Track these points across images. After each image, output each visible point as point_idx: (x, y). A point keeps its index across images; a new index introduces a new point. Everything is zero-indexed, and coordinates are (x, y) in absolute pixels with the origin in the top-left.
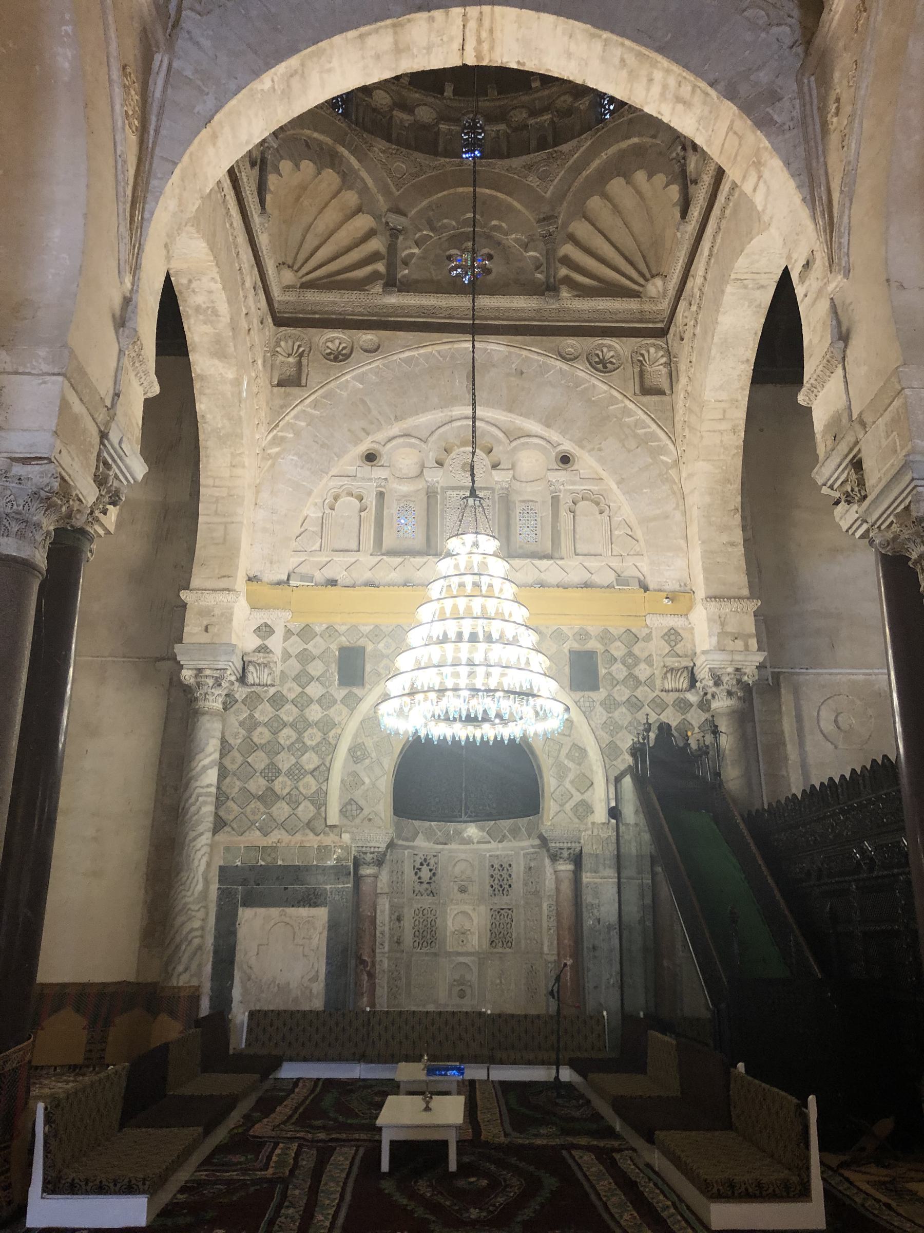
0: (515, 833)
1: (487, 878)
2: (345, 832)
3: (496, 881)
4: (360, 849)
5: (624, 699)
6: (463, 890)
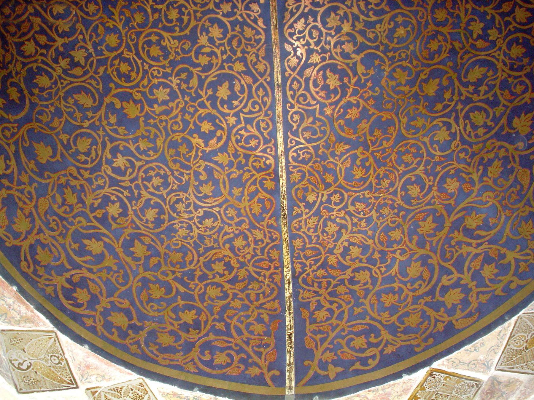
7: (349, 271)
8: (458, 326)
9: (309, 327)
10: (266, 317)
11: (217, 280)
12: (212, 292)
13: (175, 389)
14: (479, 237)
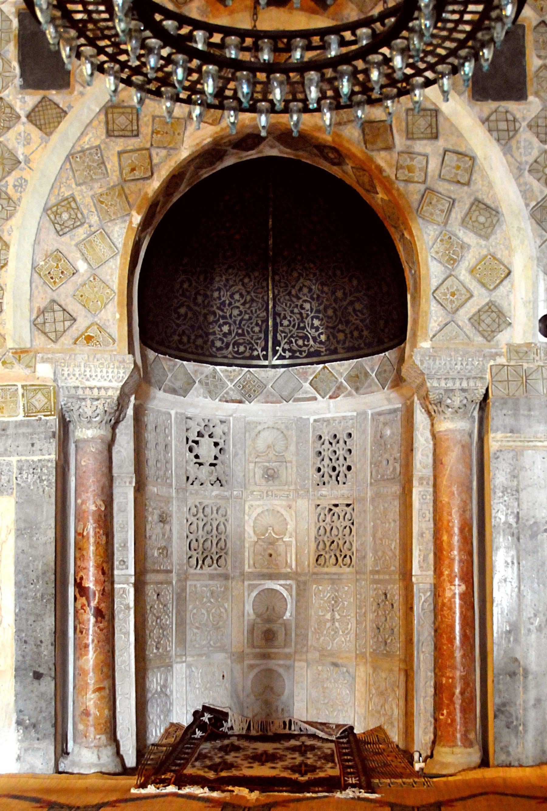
0: (357, 381)
1: (311, 454)
2: (43, 361)
3: (327, 461)
4: (73, 391)
6: (271, 476)
7: (301, 301)
8: (340, 350)
9: (280, 328)
10: (260, 322)
11: (237, 304)
12: (236, 312)
13: (225, 367)
14: (357, 315)
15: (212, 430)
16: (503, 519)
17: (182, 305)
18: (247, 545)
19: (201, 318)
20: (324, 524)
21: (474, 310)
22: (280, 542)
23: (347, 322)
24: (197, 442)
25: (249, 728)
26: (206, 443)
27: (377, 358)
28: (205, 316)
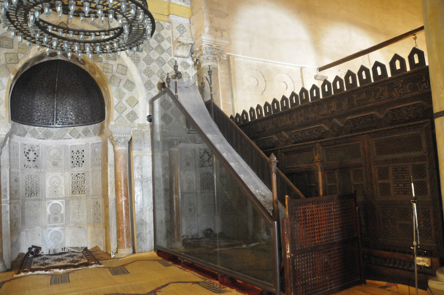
0: (86, 133)
3: (75, 159)
5: (156, 58)
6: (55, 164)
8: (80, 122)
9: (58, 115)
15: (33, 149)
16: (137, 177)
17: (23, 105)
18: (47, 188)
19: (30, 110)
20: (74, 180)
21: (127, 113)
22: (59, 187)
23: (82, 114)
24: (28, 153)
25: (49, 252)
26: (31, 153)
27: (92, 125)
28: (31, 110)
